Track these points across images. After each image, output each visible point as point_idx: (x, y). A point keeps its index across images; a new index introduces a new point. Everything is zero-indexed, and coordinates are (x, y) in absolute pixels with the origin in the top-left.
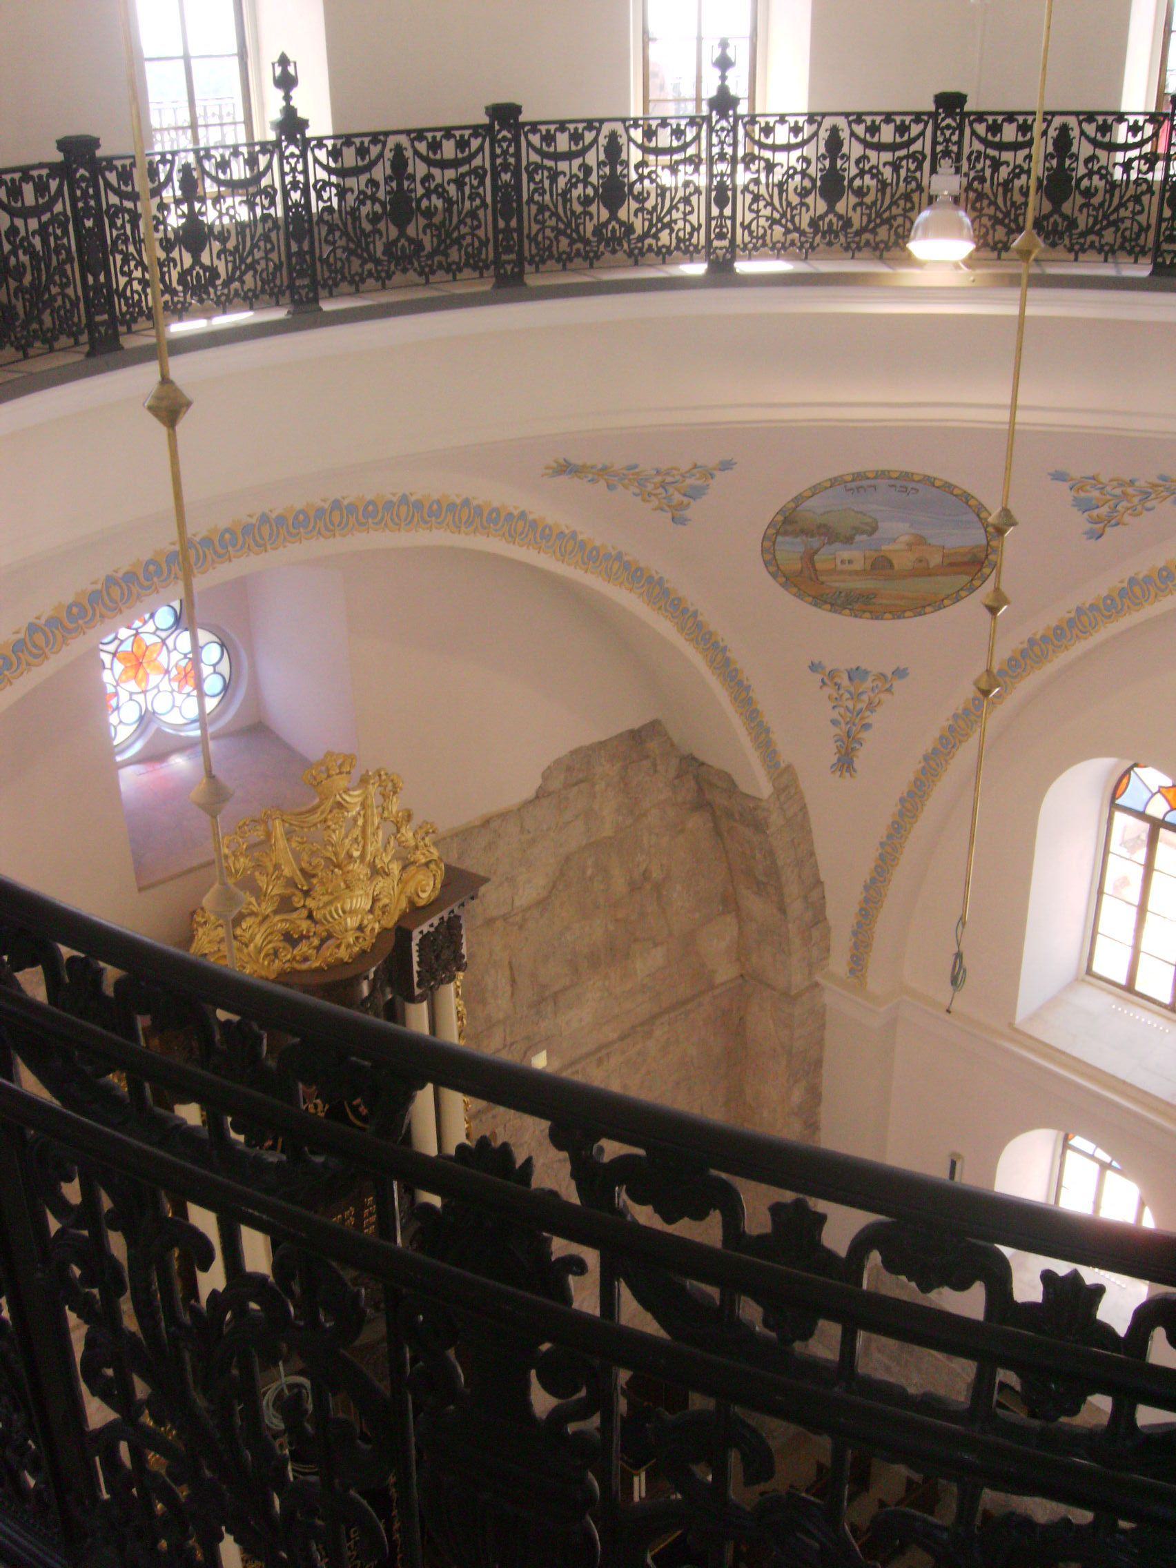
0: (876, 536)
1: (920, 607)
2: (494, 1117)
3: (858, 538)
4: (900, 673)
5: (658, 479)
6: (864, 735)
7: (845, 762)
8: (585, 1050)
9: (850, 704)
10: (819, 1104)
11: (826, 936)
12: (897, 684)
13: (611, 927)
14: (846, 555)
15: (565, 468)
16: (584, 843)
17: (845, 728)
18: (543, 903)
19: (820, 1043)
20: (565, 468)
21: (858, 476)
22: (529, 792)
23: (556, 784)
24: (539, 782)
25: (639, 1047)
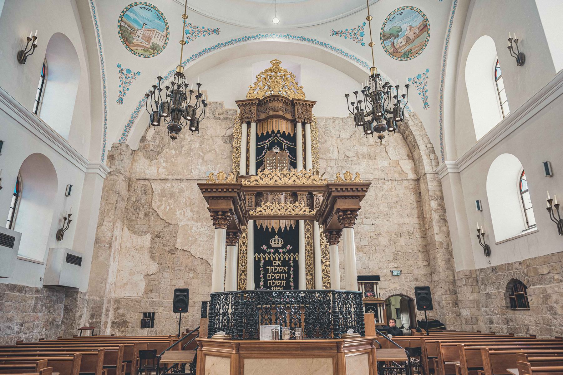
0: (402, 31)
1: (422, 47)
3: (399, 34)
4: (427, 71)
5: (353, 33)
6: (427, 94)
7: (426, 105)
9: (421, 87)
10: (445, 212)
12: (428, 74)
14: (399, 41)
15: (334, 33)
17: (422, 94)
18: (348, 139)
19: (441, 191)
20: (334, 33)
21: (390, 15)
22: (347, 116)
25: (381, 185)
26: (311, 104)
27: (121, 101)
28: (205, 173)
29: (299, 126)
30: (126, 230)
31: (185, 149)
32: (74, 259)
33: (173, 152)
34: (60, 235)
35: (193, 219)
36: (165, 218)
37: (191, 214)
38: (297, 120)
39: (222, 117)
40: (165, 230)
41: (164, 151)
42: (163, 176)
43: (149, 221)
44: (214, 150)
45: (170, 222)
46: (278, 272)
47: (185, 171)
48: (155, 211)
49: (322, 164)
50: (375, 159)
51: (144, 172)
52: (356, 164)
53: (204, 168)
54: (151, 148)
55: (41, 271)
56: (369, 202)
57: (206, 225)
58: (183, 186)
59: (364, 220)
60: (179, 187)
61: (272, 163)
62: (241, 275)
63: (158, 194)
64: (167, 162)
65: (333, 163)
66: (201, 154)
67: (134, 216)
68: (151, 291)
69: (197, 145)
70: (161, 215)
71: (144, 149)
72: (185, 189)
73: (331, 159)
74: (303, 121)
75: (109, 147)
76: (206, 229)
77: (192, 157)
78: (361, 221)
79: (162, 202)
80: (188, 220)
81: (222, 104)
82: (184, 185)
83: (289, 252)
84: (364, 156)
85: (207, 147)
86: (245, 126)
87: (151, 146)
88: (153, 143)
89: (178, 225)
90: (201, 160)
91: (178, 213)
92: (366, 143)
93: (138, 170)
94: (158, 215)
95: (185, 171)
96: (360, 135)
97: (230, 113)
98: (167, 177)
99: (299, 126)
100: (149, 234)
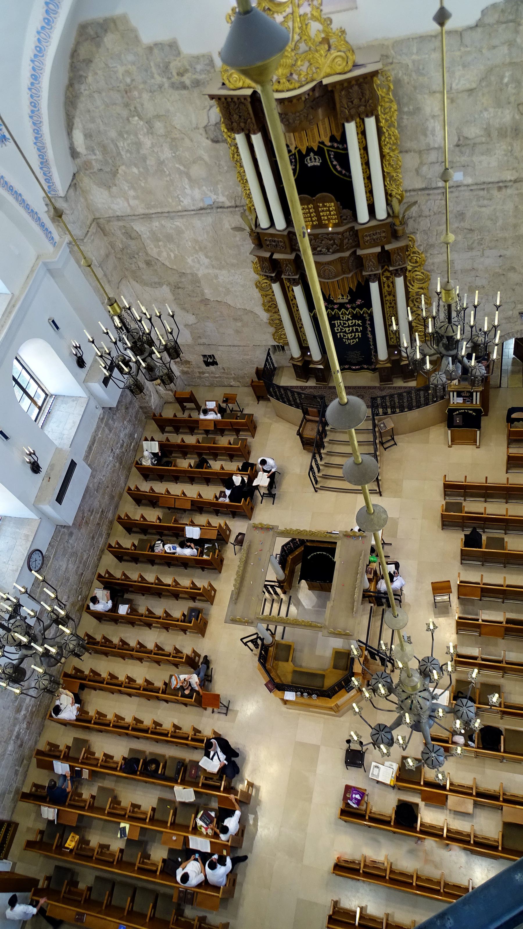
2: (429, 195)
8: (490, 180)
13: (517, 117)
16: (508, 60)
18: (471, 91)
22: (472, 21)
23: (490, 20)
24: (478, 16)
28: (202, 200)
30: (134, 283)
31: (151, 162)
33: (135, 170)
34: (81, 363)
35: (213, 267)
36: (175, 267)
37: (208, 260)
39: (187, 80)
40: (183, 280)
41: (120, 171)
42: (141, 210)
43: (156, 270)
44: (201, 158)
46: (349, 326)
47: (170, 200)
49: (409, 161)
51: (110, 208)
52: (482, 154)
53: (197, 193)
54: (96, 166)
55: (93, 404)
56: (500, 223)
57: (236, 273)
58: (178, 224)
59: (487, 252)
60: (174, 226)
62: (301, 328)
63: (149, 238)
64: (135, 189)
65: (433, 156)
66: (182, 168)
67: (133, 266)
69: (167, 153)
70: (167, 263)
71: (86, 170)
72: (183, 228)
73: (429, 149)
76: (237, 277)
77: (169, 175)
78: (479, 253)
79: (159, 247)
80: (207, 267)
81: (173, 46)
82: (179, 223)
83: (361, 307)
84: (502, 133)
85: (187, 154)
86: (240, 139)
87: (94, 163)
88: (94, 157)
89: (196, 275)
90: (186, 180)
91: (189, 260)
92: (512, 99)
93: (100, 206)
95: (170, 200)
96: (502, 78)
97: (199, 67)
98: (147, 211)
100: (165, 286)
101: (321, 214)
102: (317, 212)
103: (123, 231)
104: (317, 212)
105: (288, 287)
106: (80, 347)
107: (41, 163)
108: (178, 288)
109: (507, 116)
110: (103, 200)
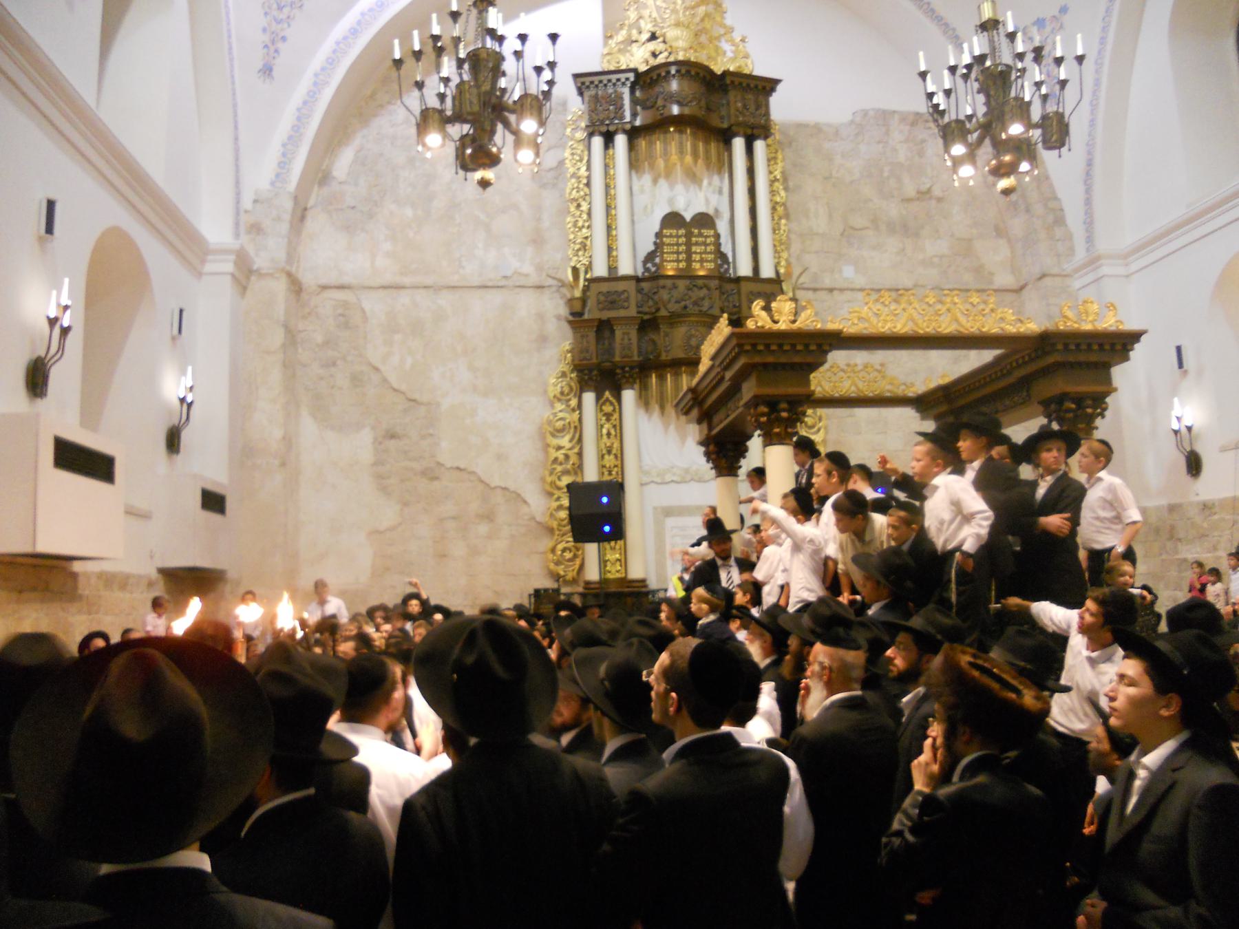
11: (1069, 237)
24: (850, 118)
26: (768, 86)
27: (267, 71)
29: (738, 144)
32: (213, 502)
33: (409, 212)
36: (403, 387)
38: (734, 128)
42: (388, 278)
45: (416, 396)
48: (377, 369)
50: (917, 235)
61: (678, 245)
66: (482, 217)
68: (388, 569)
74: (749, 132)
75: (247, 204)
82: (445, 300)
84: (891, 228)
86: (598, 141)
89: (438, 405)
94: (385, 380)
99: (738, 144)
101: (694, 249)
102: (689, 244)
103: (340, 311)
104: (689, 244)
105: (602, 426)
106: (190, 405)
107: (290, 138)
108: (393, 436)
109: (894, 210)
110: (328, 253)
